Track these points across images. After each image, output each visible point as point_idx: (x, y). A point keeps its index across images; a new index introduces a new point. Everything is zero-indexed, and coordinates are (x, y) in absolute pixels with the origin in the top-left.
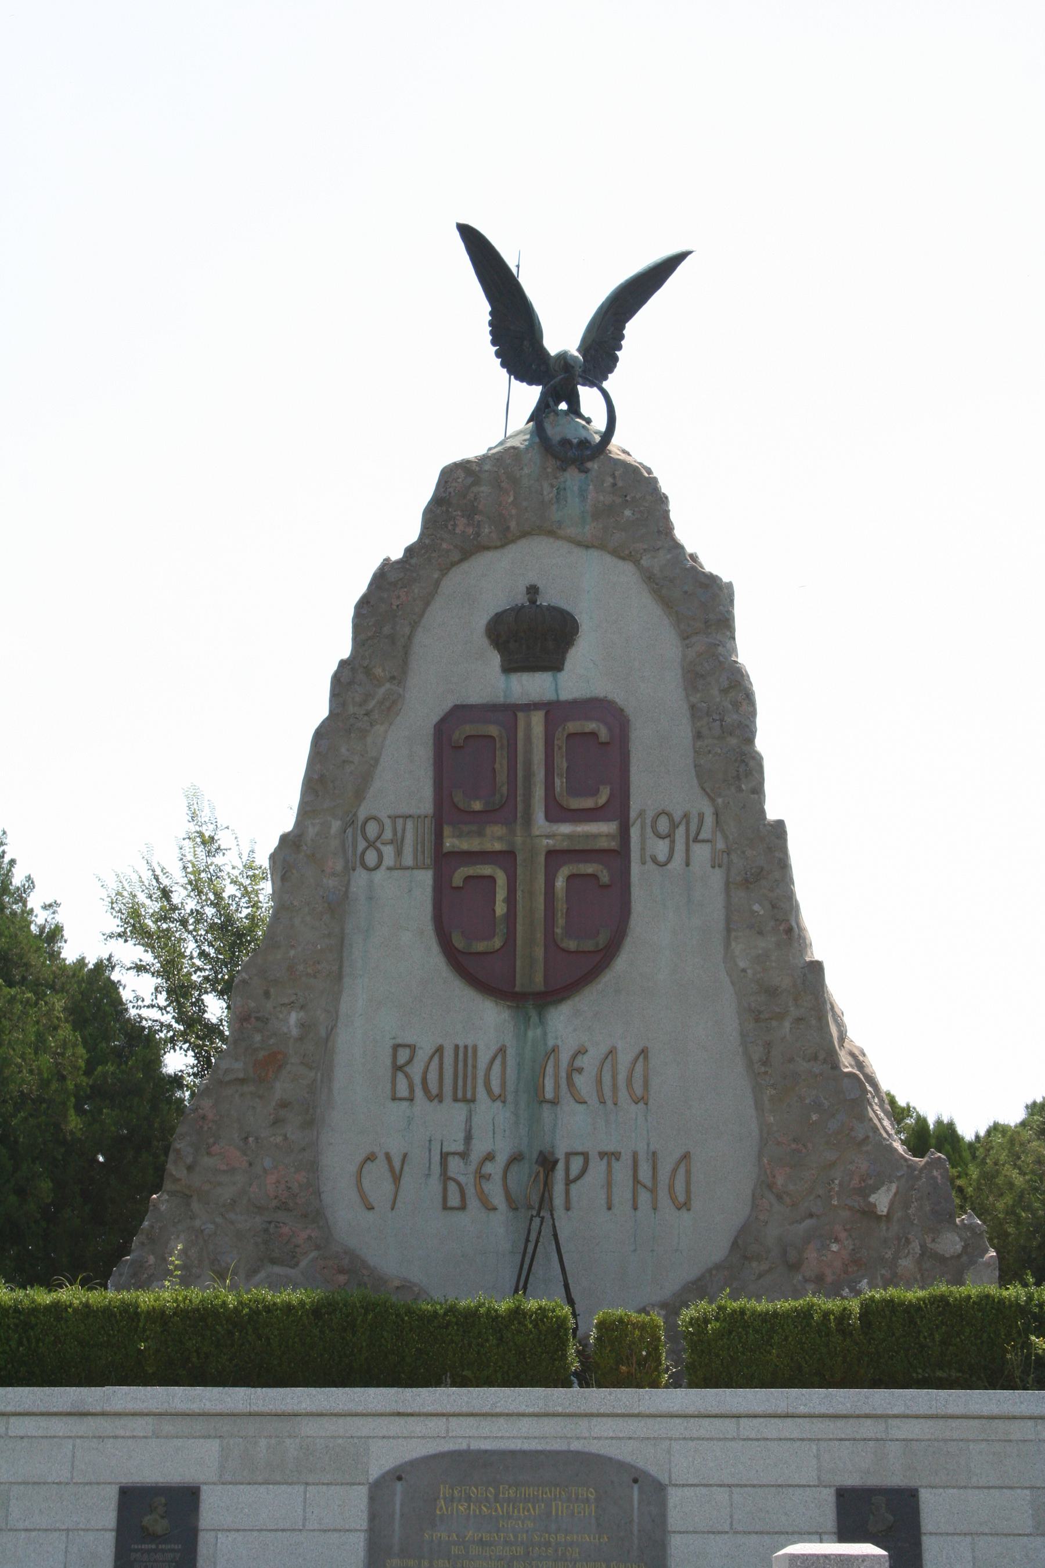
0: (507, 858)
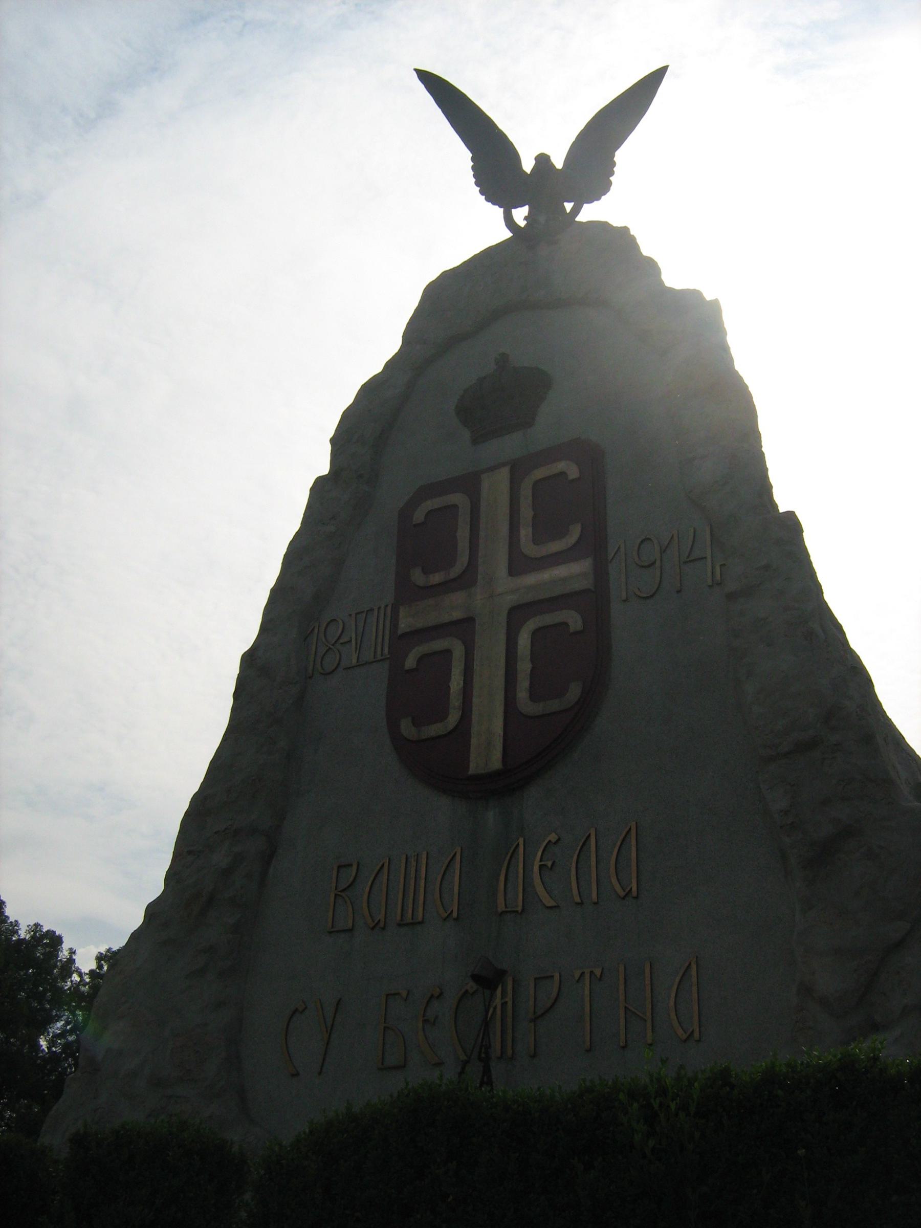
0: (464, 627)
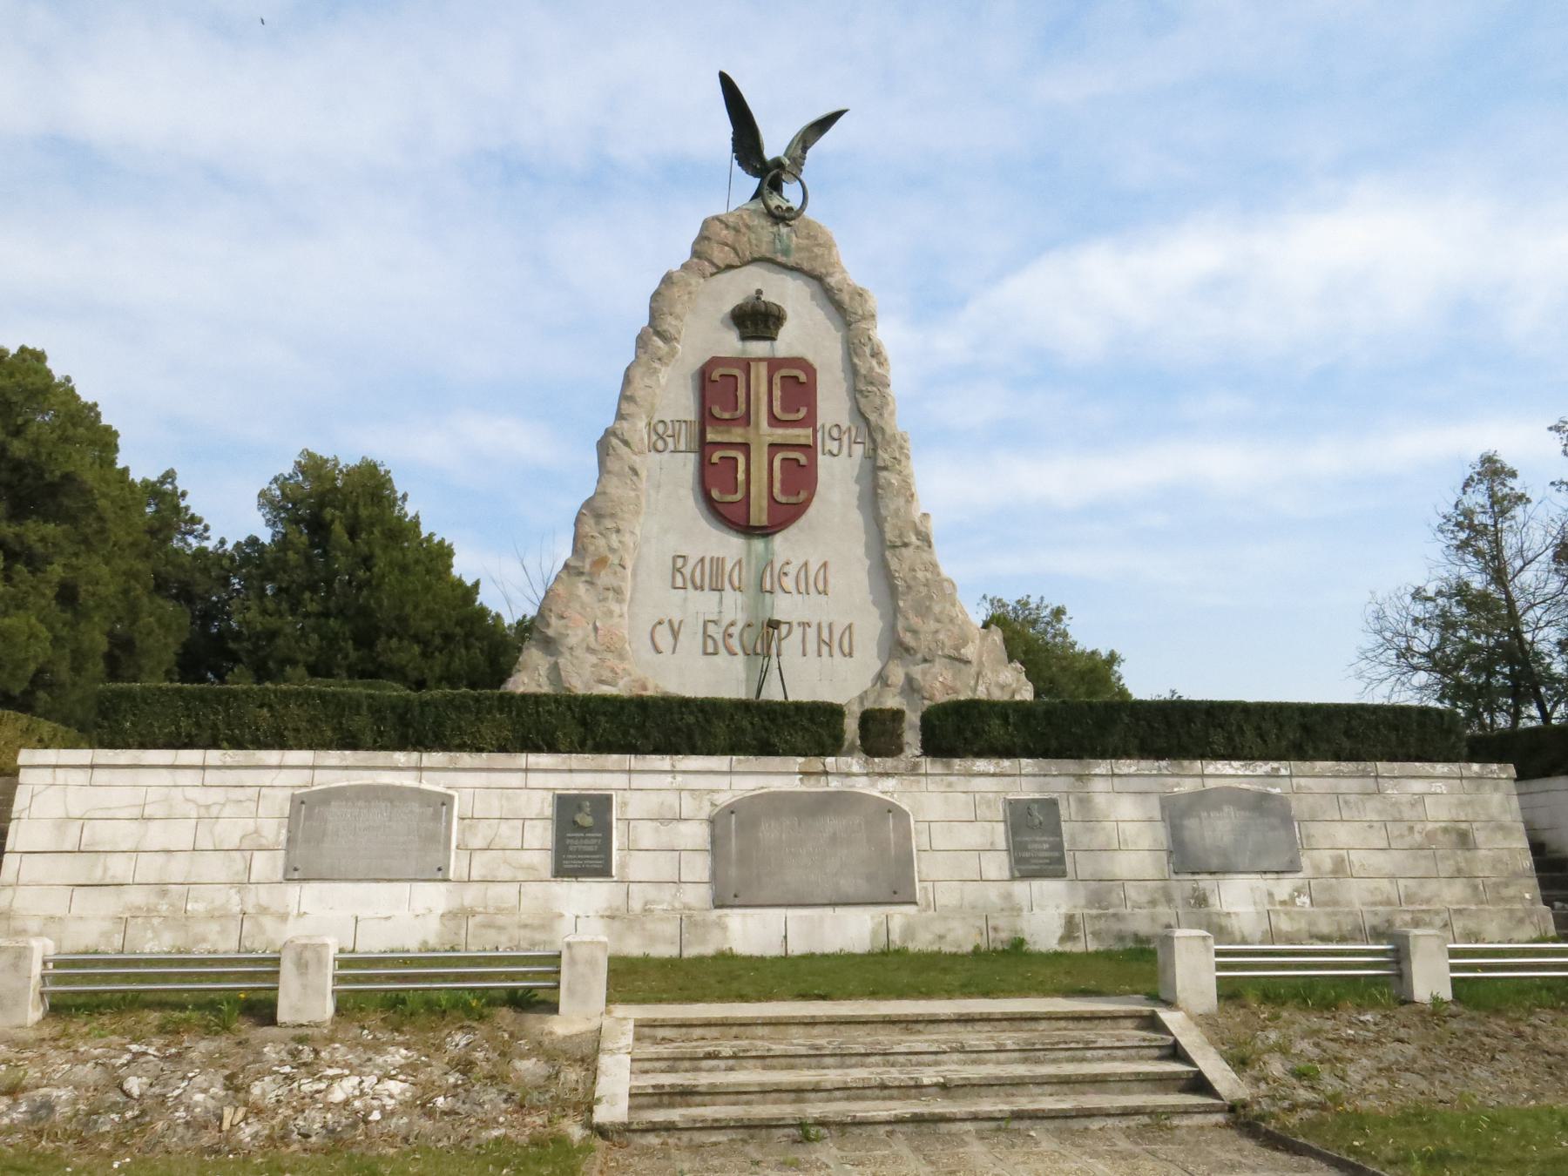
0: (745, 447)
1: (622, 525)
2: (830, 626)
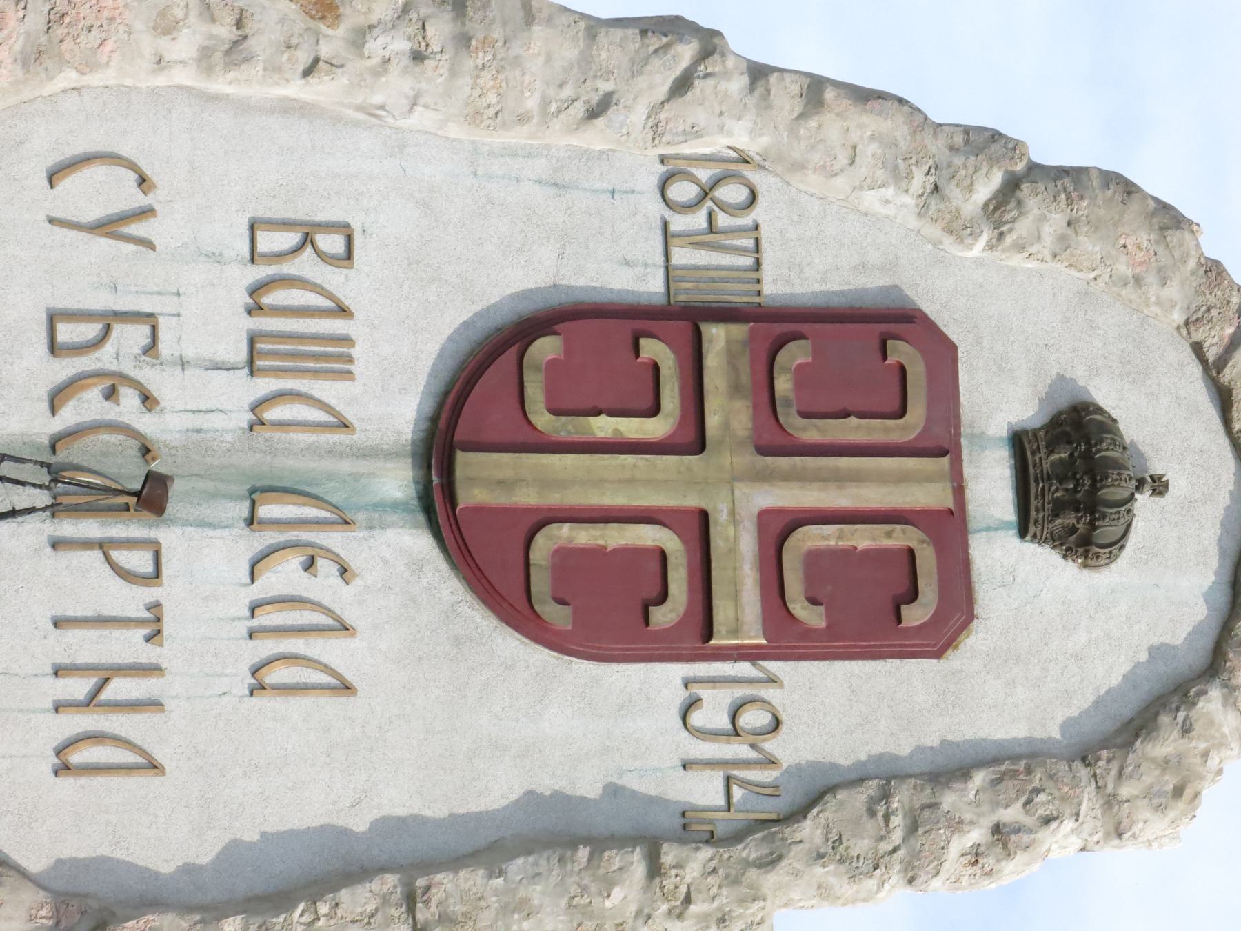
0: (693, 439)
1: (435, 72)
2: (154, 705)
